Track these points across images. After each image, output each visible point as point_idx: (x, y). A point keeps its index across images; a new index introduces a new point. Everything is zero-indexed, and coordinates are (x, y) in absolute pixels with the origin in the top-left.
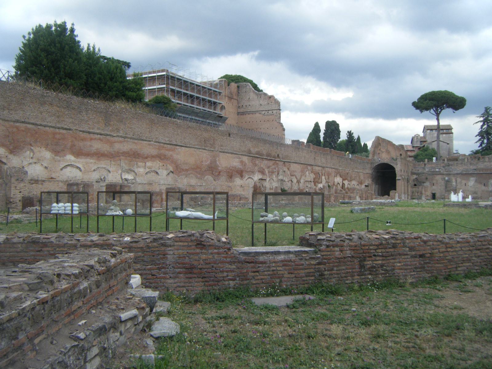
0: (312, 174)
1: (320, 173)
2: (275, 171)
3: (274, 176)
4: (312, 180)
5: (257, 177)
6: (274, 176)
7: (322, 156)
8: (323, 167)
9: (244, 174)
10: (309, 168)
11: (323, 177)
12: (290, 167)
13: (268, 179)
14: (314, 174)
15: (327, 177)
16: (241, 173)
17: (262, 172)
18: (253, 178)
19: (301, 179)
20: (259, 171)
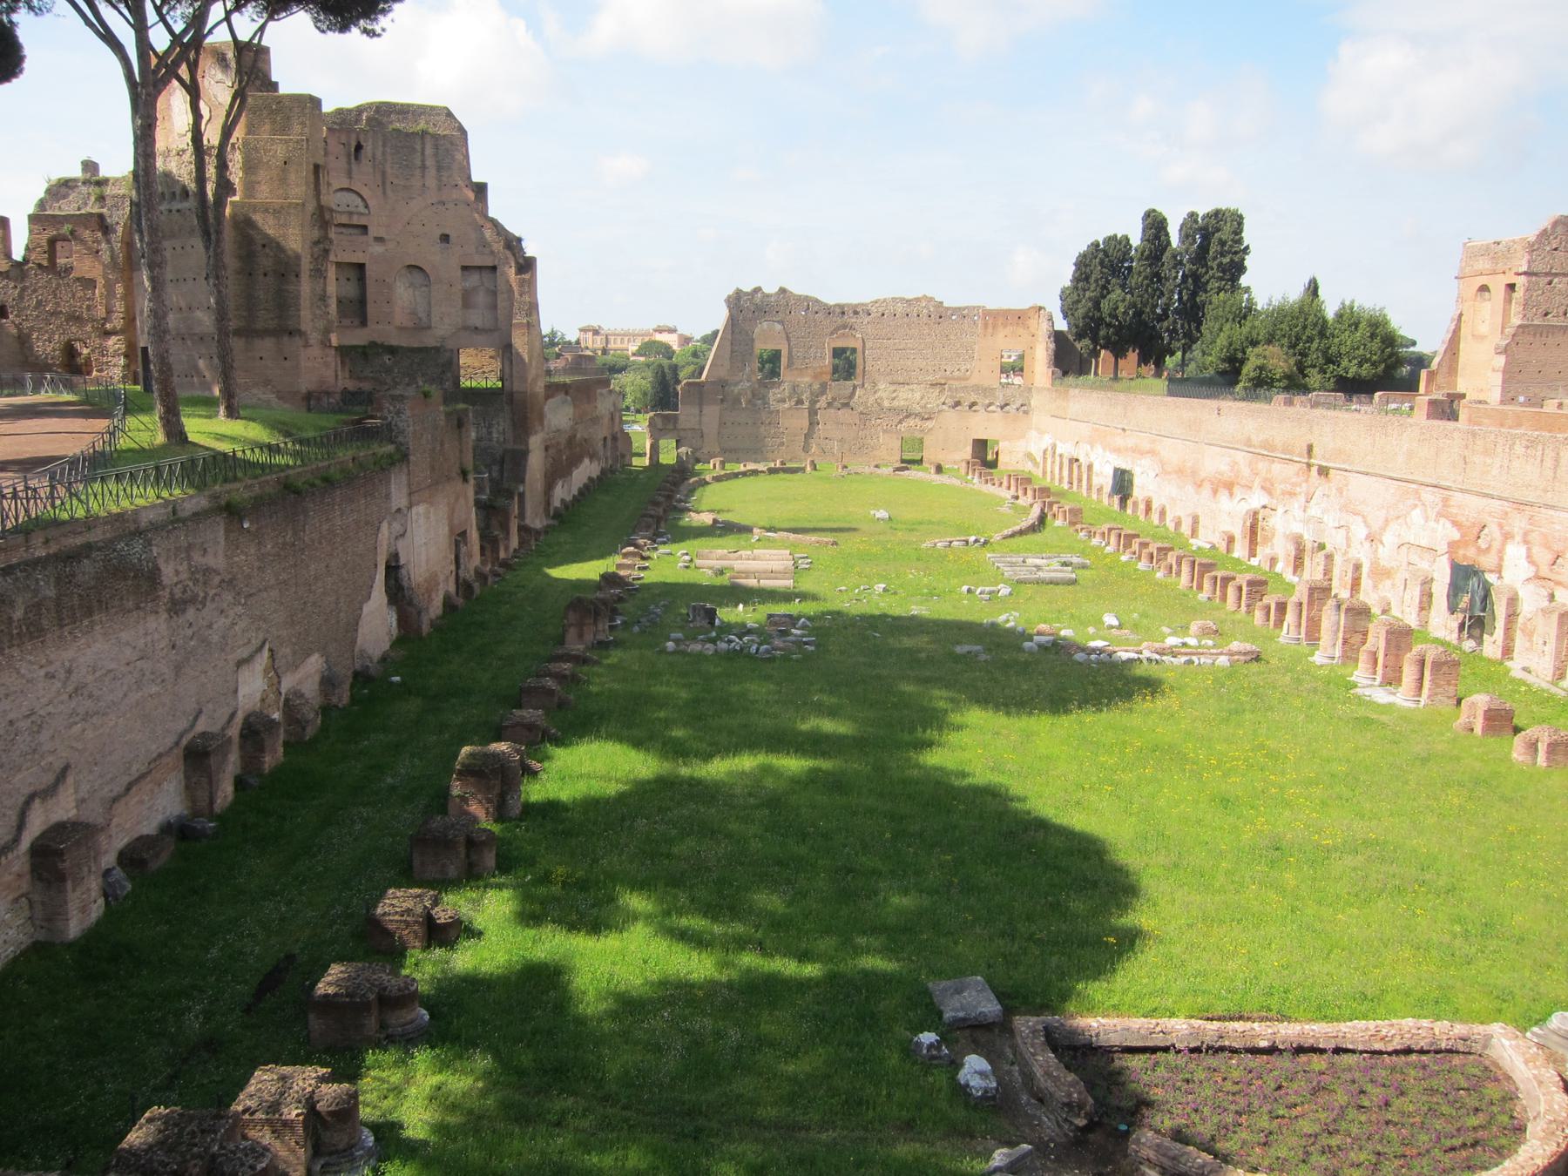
0: (1442, 520)
1: (1493, 530)
2: (1300, 493)
3: (1296, 505)
4: (1444, 548)
5: (1257, 500)
6: (1296, 505)
7: (1519, 449)
8: (1520, 505)
9: (1236, 490)
10: (1428, 495)
11: (1515, 553)
12: (1347, 485)
13: (1280, 510)
14: (1456, 524)
15: (1544, 557)
16: (1230, 487)
17: (1267, 489)
18: (1250, 500)
19: (1383, 529)
20: (1262, 487)
